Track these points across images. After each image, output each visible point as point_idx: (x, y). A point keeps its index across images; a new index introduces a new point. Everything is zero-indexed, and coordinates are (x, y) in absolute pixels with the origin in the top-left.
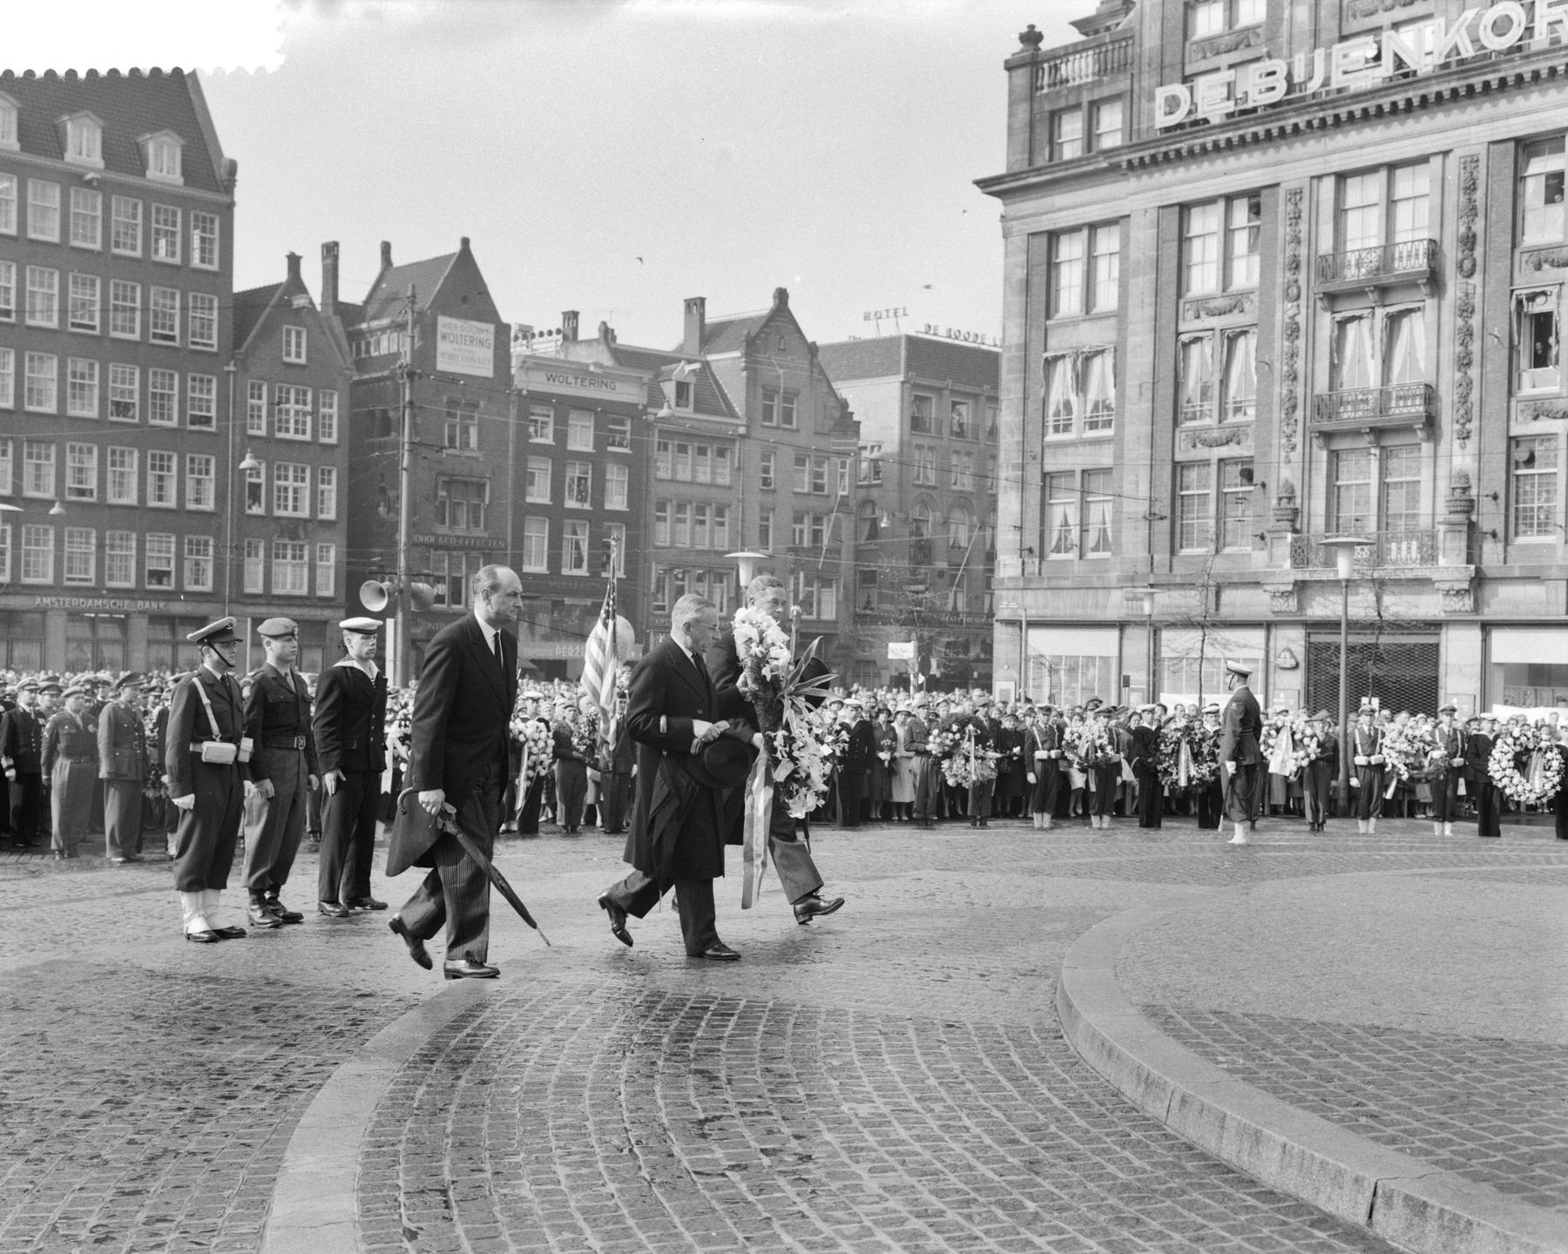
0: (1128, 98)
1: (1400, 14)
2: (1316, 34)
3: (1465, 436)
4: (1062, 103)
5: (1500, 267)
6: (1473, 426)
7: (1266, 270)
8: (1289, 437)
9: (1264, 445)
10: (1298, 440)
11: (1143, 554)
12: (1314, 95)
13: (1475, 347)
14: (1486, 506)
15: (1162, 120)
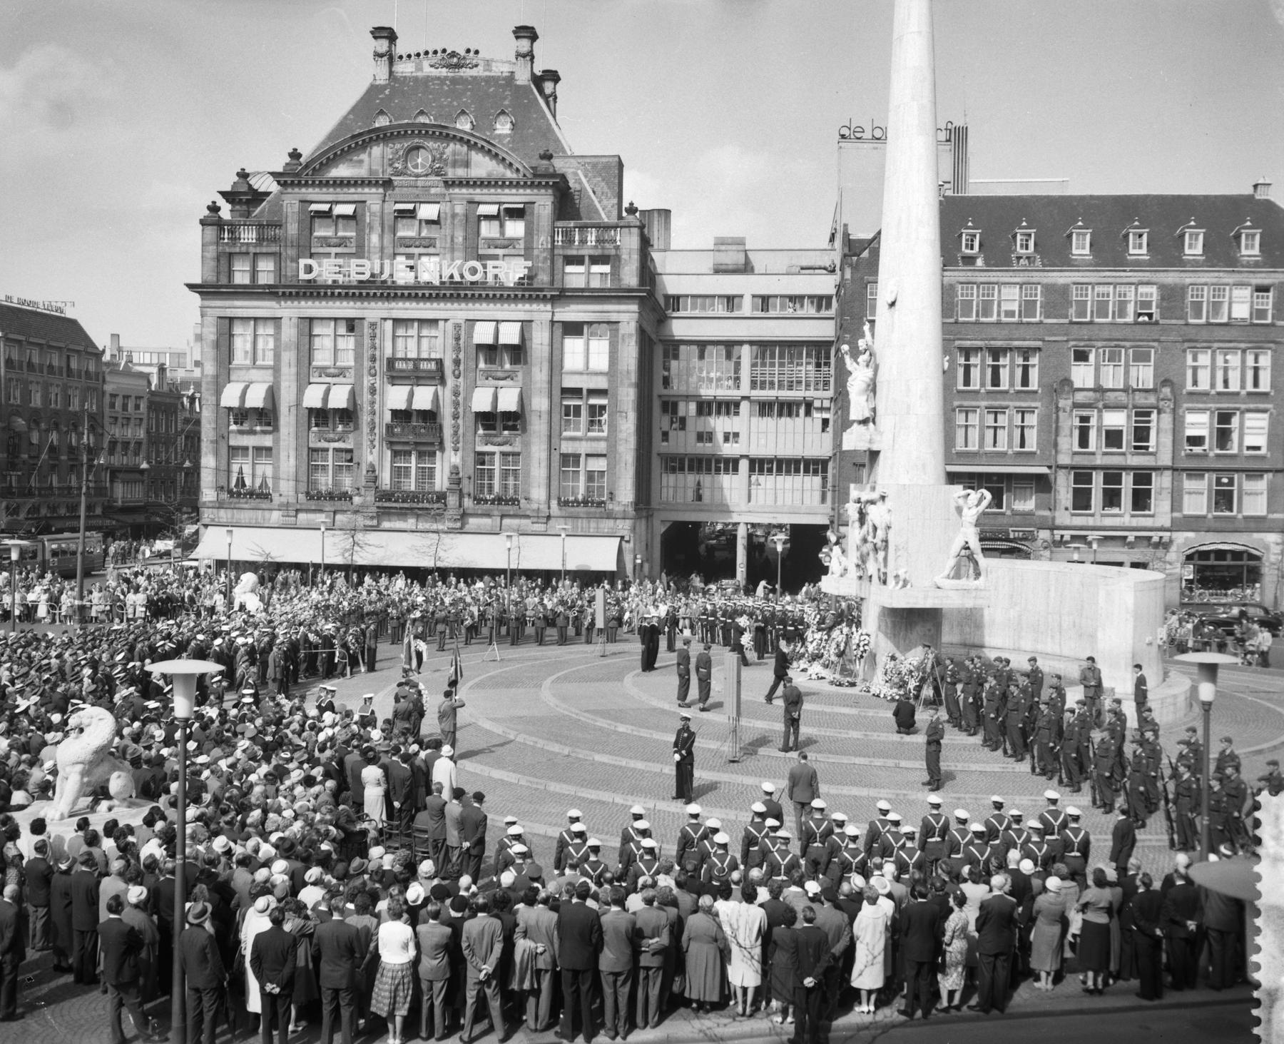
0: (277, 256)
1: (422, 250)
2: (382, 249)
3: (456, 450)
4: (237, 250)
5: (472, 375)
6: (460, 445)
7: (358, 357)
8: (372, 442)
9: (359, 444)
10: (376, 443)
11: (292, 493)
12: (385, 282)
13: (461, 410)
14: (465, 482)
15: (303, 276)
